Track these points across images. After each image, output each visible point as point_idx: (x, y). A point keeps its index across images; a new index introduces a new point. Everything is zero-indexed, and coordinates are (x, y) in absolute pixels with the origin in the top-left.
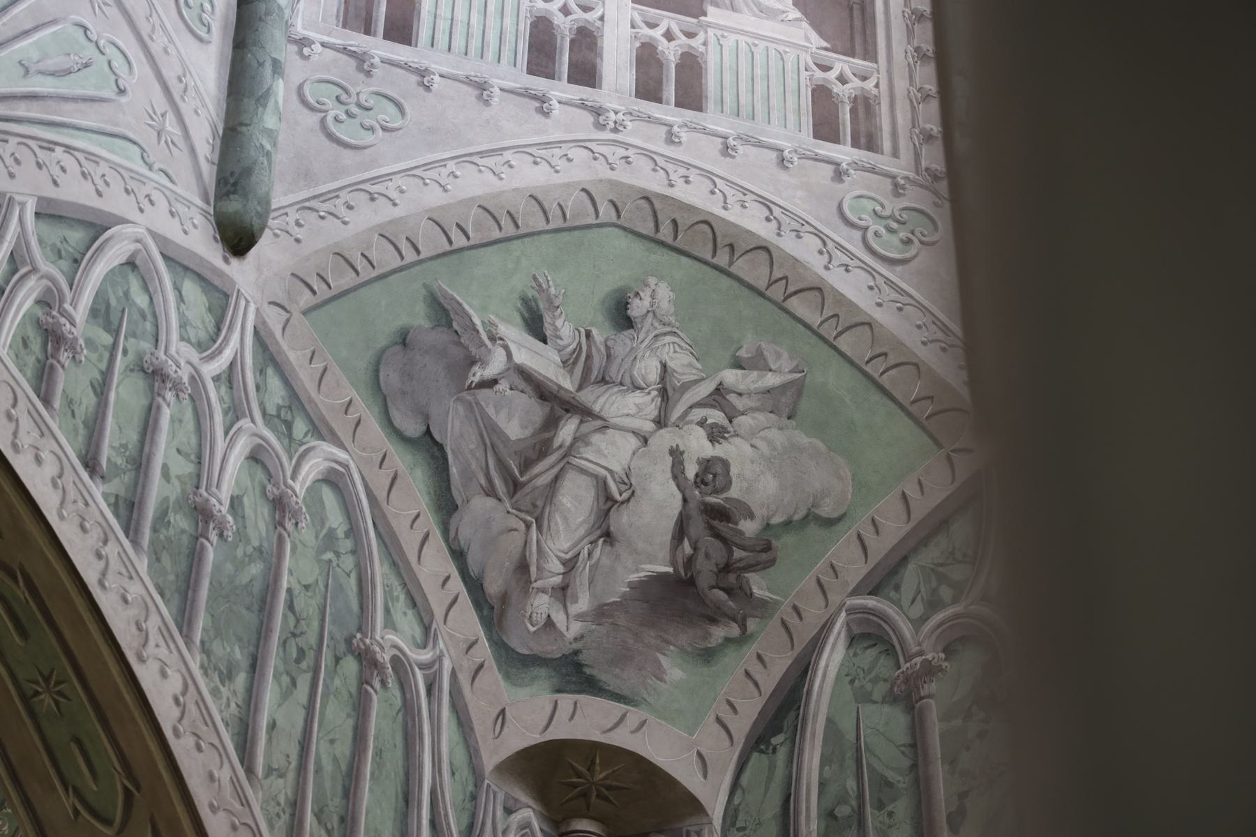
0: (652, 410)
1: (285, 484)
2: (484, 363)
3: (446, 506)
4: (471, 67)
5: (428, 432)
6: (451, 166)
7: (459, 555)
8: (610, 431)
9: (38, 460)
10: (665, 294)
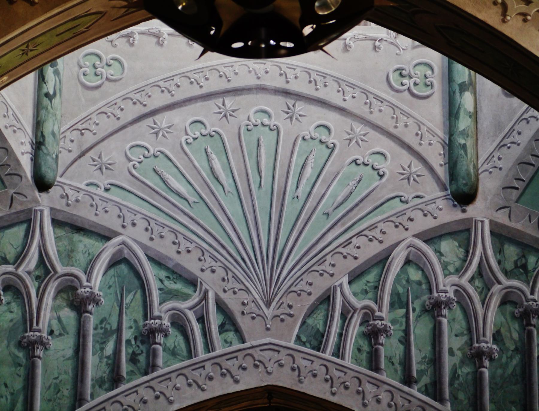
1: (527, 300)
9: (378, 401)
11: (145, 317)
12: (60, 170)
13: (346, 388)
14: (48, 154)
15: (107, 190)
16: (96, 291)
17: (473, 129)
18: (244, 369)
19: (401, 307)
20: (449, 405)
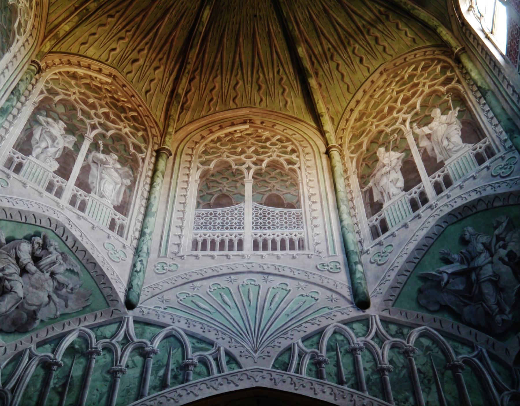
0: (488, 255)
1: (406, 346)
2: (443, 280)
3: (457, 316)
4: (402, 223)
5: (441, 306)
6: (406, 247)
7: (469, 324)
8: (483, 268)
9: (324, 392)
10: (470, 229)
11: (183, 359)
12: (140, 302)
13: (304, 387)
14: (134, 291)
15: (165, 309)
16: (156, 348)
17: (363, 276)
18: (242, 380)
19: (333, 350)
20: (367, 393)
